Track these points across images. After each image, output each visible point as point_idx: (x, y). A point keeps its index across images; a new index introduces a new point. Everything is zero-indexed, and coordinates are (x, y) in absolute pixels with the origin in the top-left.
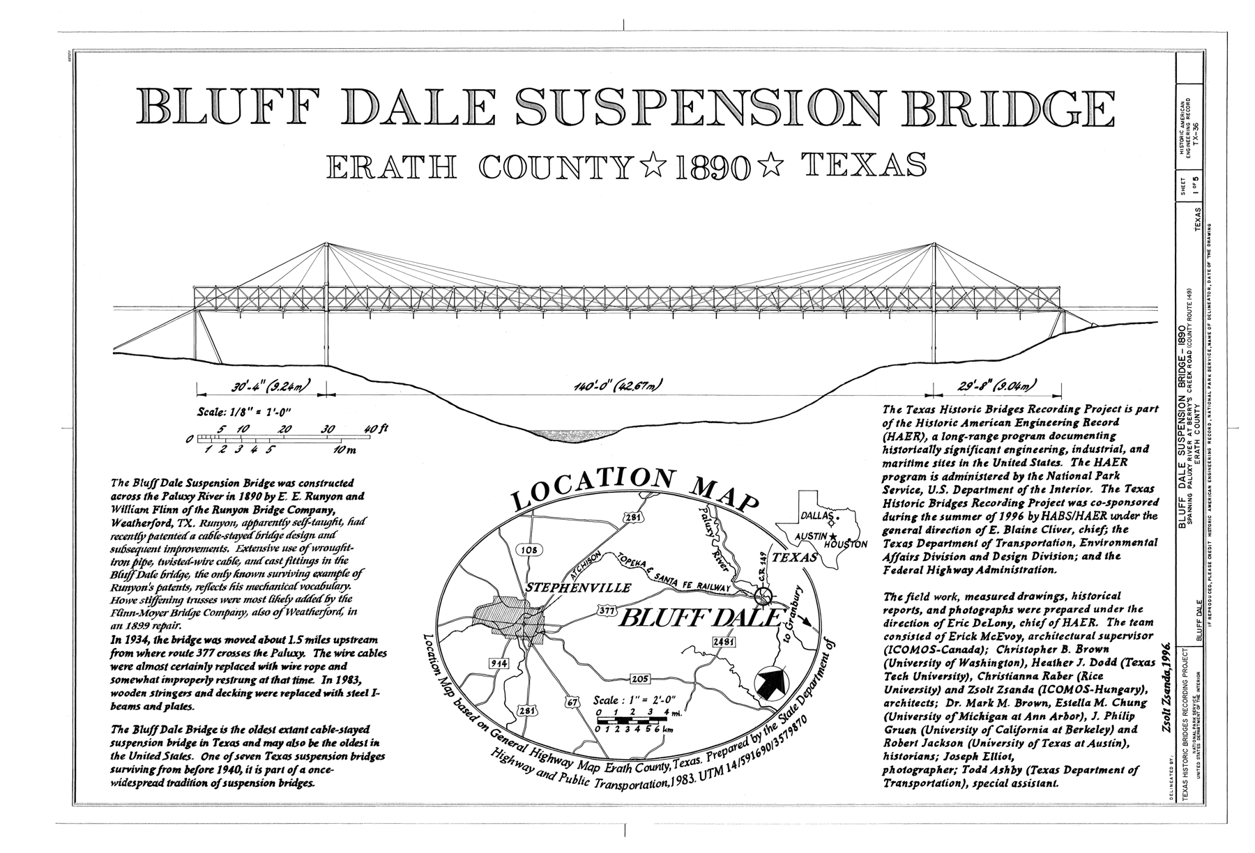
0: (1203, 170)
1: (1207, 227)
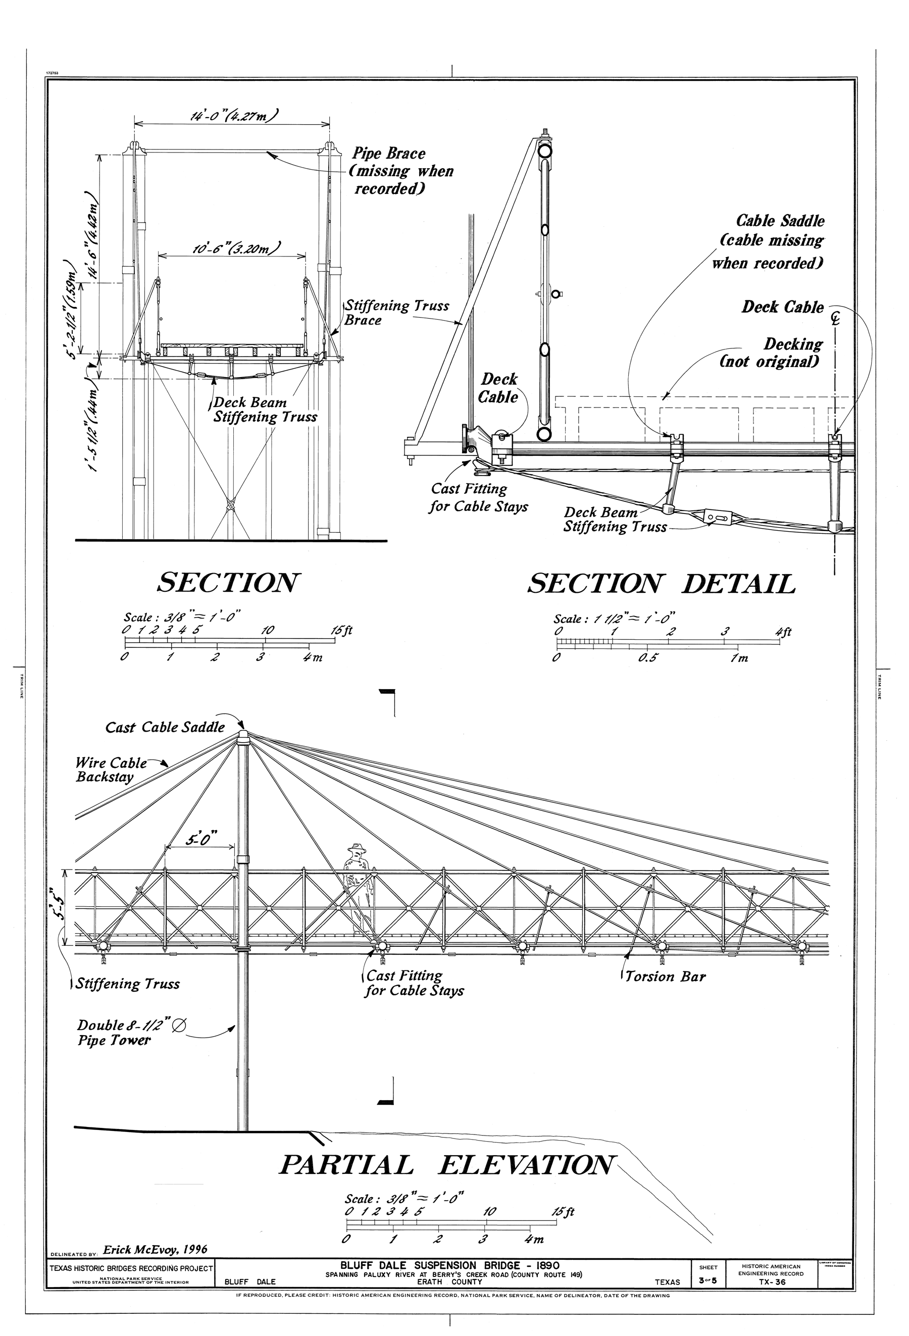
0: (215, 1287)
1: (453, 1293)
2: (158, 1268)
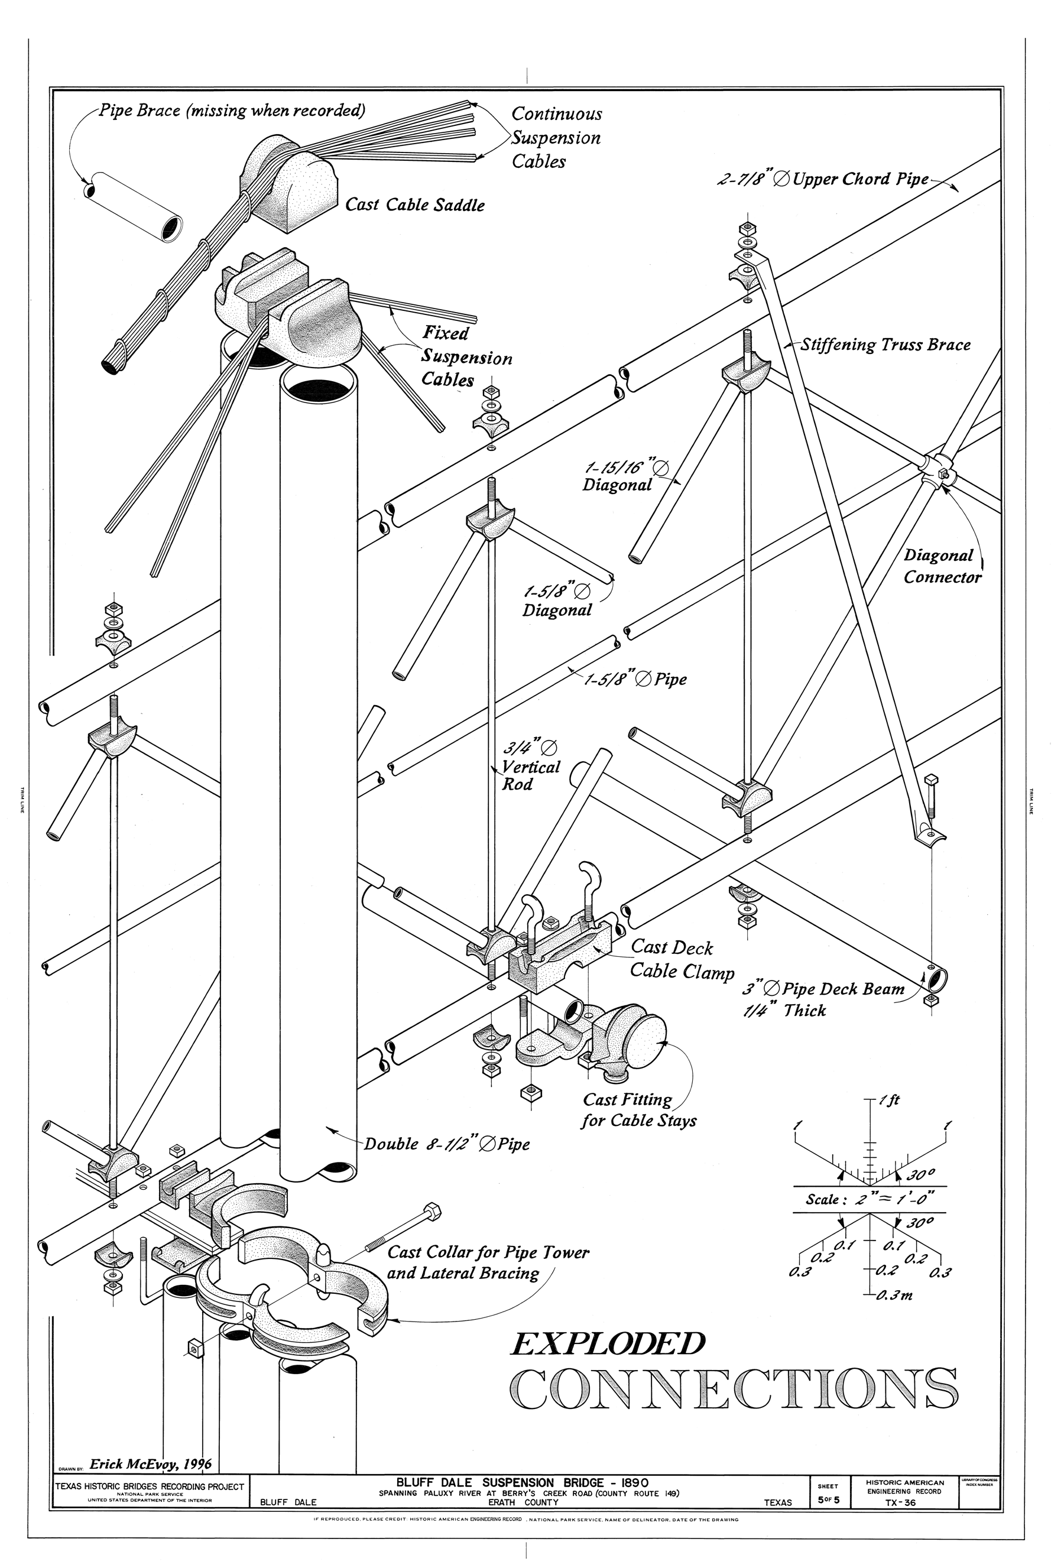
2: (991, 1480)
